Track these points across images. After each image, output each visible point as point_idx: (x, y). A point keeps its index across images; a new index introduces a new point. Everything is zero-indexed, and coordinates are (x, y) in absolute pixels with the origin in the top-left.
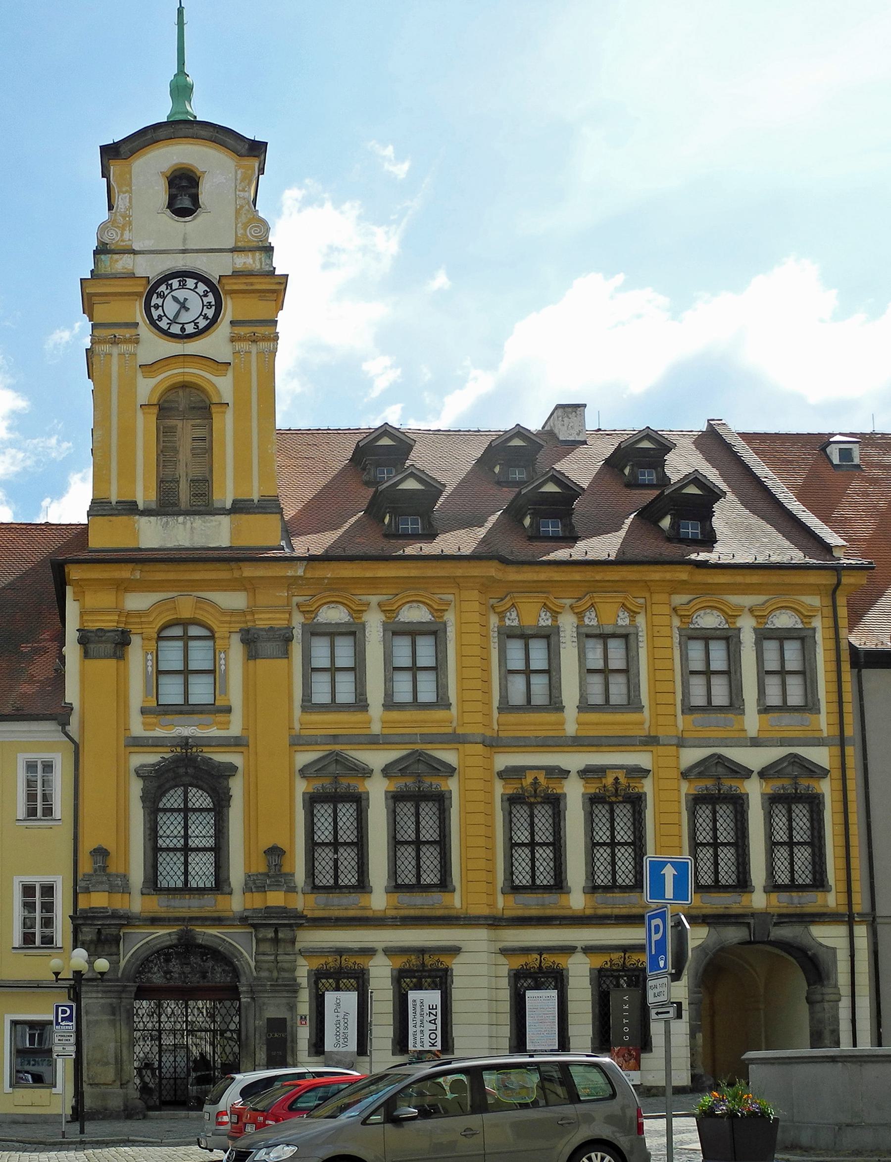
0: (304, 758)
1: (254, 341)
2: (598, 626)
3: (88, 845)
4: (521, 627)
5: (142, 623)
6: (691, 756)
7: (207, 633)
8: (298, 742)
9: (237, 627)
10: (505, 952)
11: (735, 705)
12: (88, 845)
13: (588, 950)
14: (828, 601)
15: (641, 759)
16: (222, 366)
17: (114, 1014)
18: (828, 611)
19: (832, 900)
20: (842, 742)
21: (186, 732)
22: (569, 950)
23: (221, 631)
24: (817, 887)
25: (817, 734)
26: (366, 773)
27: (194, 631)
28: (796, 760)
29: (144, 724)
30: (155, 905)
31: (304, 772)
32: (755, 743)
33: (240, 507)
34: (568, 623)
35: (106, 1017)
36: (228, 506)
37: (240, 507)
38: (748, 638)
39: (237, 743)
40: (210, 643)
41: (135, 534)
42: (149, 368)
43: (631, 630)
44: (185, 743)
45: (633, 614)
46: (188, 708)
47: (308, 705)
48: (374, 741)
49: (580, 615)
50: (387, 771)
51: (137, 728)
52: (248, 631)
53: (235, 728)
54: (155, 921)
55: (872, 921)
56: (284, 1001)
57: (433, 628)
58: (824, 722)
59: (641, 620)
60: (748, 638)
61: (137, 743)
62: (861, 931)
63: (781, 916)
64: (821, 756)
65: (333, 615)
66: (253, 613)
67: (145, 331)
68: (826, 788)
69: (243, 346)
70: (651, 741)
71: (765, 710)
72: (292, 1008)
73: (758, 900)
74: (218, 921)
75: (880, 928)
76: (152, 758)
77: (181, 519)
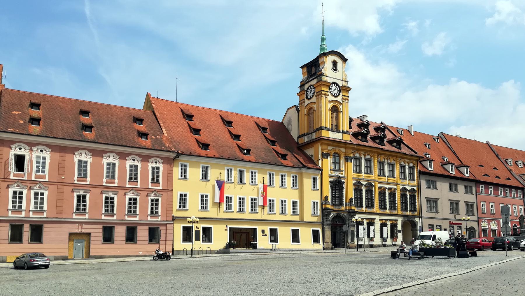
0: (354, 182)
1: (346, 100)
2: (390, 162)
3: (324, 195)
4: (380, 161)
5: (330, 152)
6: (401, 187)
7: (338, 156)
8: (354, 179)
9: (345, 155)
10: (380, 220)
11: (405, 178)
12: (324, 195)
13: (390, 220)
14: (416, 162)
15: (395, 187)
16: (341, 104)
17: (329, 229)
18: (416, 164)
19: (417, 214)
20: (418, 187)
21: (337, 174)
22: (387, 220)
23: (342, 156)
24: (415, 211)
25: (415, 185)
26: (362, 185)
27: (336, 155)
28: (414, 189)
29: (331, 172)
30: (333, 208)
31: (354, 184)
32: (408, 186)
33: (343, 132)
34: (386, 161)
35: (328, 229)
36: (342, 131)
37: (343, 132)
38: (407, 167)
39: (344, 178)
40: (338, 158)
41: (329, 134)
42: (330, 102)
43: (394, 164)
44: (337, 176)
45: (394, 161)
46: (335, 170)
47: (354, 172)
48: (364, 180)
49: (388, 160)
50: (365, 185)
51: (330, 173)
52: (347, 157)
53: (343, 175)
54: (335, 211)
55: (422, 218)
56: (353, 227)
57: (370, 160)
58: (415, 183)
59: (395, 162)
60: (407, 167)
61: (330, 176)
62: (421, 219)
63: (412, 216)
64: (415, 188)
65: (357, 155)
66: (347, 153)
67: (330, 95)
68: (416, 194)
69: (344, 100)
70: (397, 184)
71: (409, 180)
72: (354, 229)
73: (408, 213)
74: (343, 211)
75: (423, 219)
76: (332, 179)
77: (335, 133)
